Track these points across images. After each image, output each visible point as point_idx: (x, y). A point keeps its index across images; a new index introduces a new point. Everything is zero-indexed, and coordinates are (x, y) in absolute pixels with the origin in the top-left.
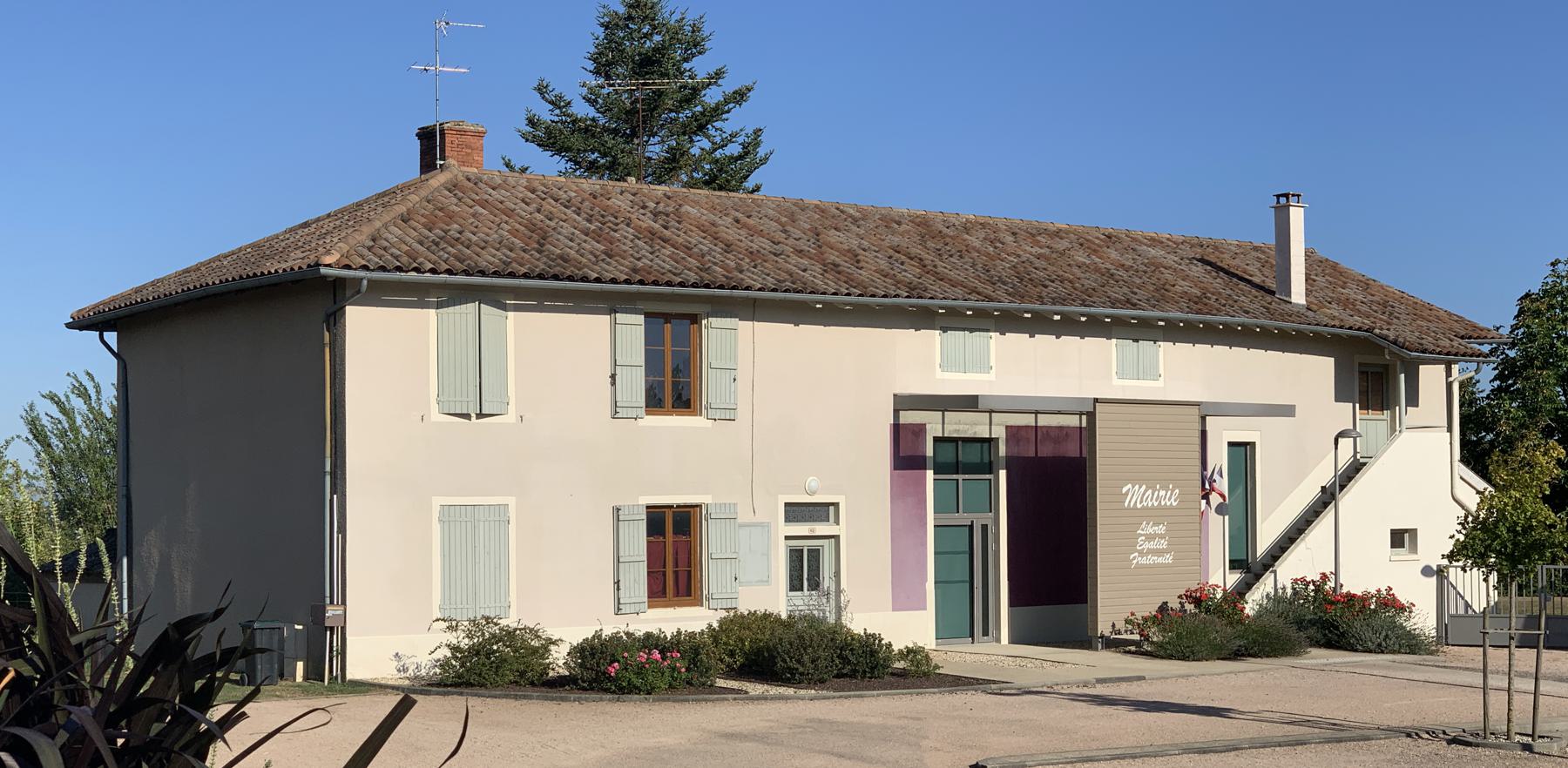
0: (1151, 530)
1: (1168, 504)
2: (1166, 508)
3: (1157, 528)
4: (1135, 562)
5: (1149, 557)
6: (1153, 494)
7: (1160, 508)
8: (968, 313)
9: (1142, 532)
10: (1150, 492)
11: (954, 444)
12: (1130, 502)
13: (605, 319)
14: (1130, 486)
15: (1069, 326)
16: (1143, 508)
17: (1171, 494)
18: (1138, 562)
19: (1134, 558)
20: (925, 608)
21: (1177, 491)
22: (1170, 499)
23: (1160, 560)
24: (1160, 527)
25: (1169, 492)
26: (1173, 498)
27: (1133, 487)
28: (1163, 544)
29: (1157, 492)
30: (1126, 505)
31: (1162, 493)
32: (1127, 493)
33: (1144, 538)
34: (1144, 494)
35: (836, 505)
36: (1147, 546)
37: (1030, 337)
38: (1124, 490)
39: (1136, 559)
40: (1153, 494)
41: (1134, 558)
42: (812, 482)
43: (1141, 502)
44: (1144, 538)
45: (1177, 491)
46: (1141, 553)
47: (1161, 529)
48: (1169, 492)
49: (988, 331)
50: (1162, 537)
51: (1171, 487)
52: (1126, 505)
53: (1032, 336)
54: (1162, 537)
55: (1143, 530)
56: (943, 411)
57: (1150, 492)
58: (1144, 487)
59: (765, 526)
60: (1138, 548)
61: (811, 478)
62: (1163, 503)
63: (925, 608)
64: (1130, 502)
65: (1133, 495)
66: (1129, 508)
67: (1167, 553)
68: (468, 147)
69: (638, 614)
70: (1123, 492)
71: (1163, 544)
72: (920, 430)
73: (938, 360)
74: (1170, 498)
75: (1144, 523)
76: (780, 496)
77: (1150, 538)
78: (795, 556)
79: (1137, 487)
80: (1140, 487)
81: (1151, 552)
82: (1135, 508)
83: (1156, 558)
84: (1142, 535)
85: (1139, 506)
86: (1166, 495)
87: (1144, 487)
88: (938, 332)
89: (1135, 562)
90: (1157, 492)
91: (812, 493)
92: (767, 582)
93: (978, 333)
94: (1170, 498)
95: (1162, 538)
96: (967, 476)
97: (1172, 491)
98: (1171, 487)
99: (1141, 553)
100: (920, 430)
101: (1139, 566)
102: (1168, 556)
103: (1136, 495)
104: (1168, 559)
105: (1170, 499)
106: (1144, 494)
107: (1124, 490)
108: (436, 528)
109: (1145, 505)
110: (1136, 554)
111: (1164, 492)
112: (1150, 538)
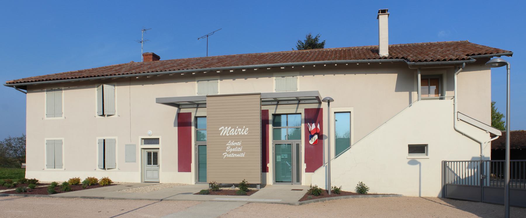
0: (233, 144)
2: (241, 135)
3: (237, 143)
4: (225, 156)
5: (232, 154)
6: (235, 130)
7: (238, 135)
9: (229, 145)
10: (233, 129)
11: (198, 118)
12: (223, 133)
14: (223, 127)
16: (230, 136)
17: (244, 130)
18: (226, 156)
19: (225, 155)
21: (247, 129)
22: (243, 132)
23: (238, 156)
25: (243, 129)
26: (245, 131)
27: (224, 128)
28: (240, 149)
29: (237, 130)
30: (221, 134)
31: (240, 130)
32: (221, 130)
33: (230, 147)
34: (230, 130)
35: (158, 139)
36: (231, 150)
37: (233, 80)
38: (220, 129)
39: (225, 155)
40: (235, 130)
41: (225, 155)
42: (150, 132)
43: (229, 133)
45: (247, 129)
46: (228, 153)
47: (239, 144)
48: (243, 129)
49: (218, 80)
50: (239, 147)
51: (244, 127)
54: (239, 147)
56: (197, 108)
57: (233, 129)
58: (230, 128)
59: (134, 146)
60: (227, 151)
61: (151, 132)
62: (240, 134)
64: (223, 133)
65: (225, 131)
66: (222, 136)
67: (242, 153)
68: (149, 58)
70: (219, 130)
71: (240, 149)
72: (190, 114)
74: (243, 131)
75: (230, 141)
76: (139, 136)
77: (232, 147)
79: (226, 128)
80: (228, 128)
81: (232, 152)
85: (227, 135)
86: (241, 130)
87: (230, 128)
88: (196, 82)
89: (225, 156)
90: (237, 130)
92: (135, 162)
93: (211, 81)
94: (243, 131)
95: (239, 147)
98: (244, 127)
99: (228, 153)
100: (190, 114)
101: (226, 158)
103: (225, 131)
104: (243, 155)
105: (243, 132)
106: (230, 130)
107: (220, 129)
109: (231, 134)
110: (226, 153)
111: (240, 130)
112: (232, 147)
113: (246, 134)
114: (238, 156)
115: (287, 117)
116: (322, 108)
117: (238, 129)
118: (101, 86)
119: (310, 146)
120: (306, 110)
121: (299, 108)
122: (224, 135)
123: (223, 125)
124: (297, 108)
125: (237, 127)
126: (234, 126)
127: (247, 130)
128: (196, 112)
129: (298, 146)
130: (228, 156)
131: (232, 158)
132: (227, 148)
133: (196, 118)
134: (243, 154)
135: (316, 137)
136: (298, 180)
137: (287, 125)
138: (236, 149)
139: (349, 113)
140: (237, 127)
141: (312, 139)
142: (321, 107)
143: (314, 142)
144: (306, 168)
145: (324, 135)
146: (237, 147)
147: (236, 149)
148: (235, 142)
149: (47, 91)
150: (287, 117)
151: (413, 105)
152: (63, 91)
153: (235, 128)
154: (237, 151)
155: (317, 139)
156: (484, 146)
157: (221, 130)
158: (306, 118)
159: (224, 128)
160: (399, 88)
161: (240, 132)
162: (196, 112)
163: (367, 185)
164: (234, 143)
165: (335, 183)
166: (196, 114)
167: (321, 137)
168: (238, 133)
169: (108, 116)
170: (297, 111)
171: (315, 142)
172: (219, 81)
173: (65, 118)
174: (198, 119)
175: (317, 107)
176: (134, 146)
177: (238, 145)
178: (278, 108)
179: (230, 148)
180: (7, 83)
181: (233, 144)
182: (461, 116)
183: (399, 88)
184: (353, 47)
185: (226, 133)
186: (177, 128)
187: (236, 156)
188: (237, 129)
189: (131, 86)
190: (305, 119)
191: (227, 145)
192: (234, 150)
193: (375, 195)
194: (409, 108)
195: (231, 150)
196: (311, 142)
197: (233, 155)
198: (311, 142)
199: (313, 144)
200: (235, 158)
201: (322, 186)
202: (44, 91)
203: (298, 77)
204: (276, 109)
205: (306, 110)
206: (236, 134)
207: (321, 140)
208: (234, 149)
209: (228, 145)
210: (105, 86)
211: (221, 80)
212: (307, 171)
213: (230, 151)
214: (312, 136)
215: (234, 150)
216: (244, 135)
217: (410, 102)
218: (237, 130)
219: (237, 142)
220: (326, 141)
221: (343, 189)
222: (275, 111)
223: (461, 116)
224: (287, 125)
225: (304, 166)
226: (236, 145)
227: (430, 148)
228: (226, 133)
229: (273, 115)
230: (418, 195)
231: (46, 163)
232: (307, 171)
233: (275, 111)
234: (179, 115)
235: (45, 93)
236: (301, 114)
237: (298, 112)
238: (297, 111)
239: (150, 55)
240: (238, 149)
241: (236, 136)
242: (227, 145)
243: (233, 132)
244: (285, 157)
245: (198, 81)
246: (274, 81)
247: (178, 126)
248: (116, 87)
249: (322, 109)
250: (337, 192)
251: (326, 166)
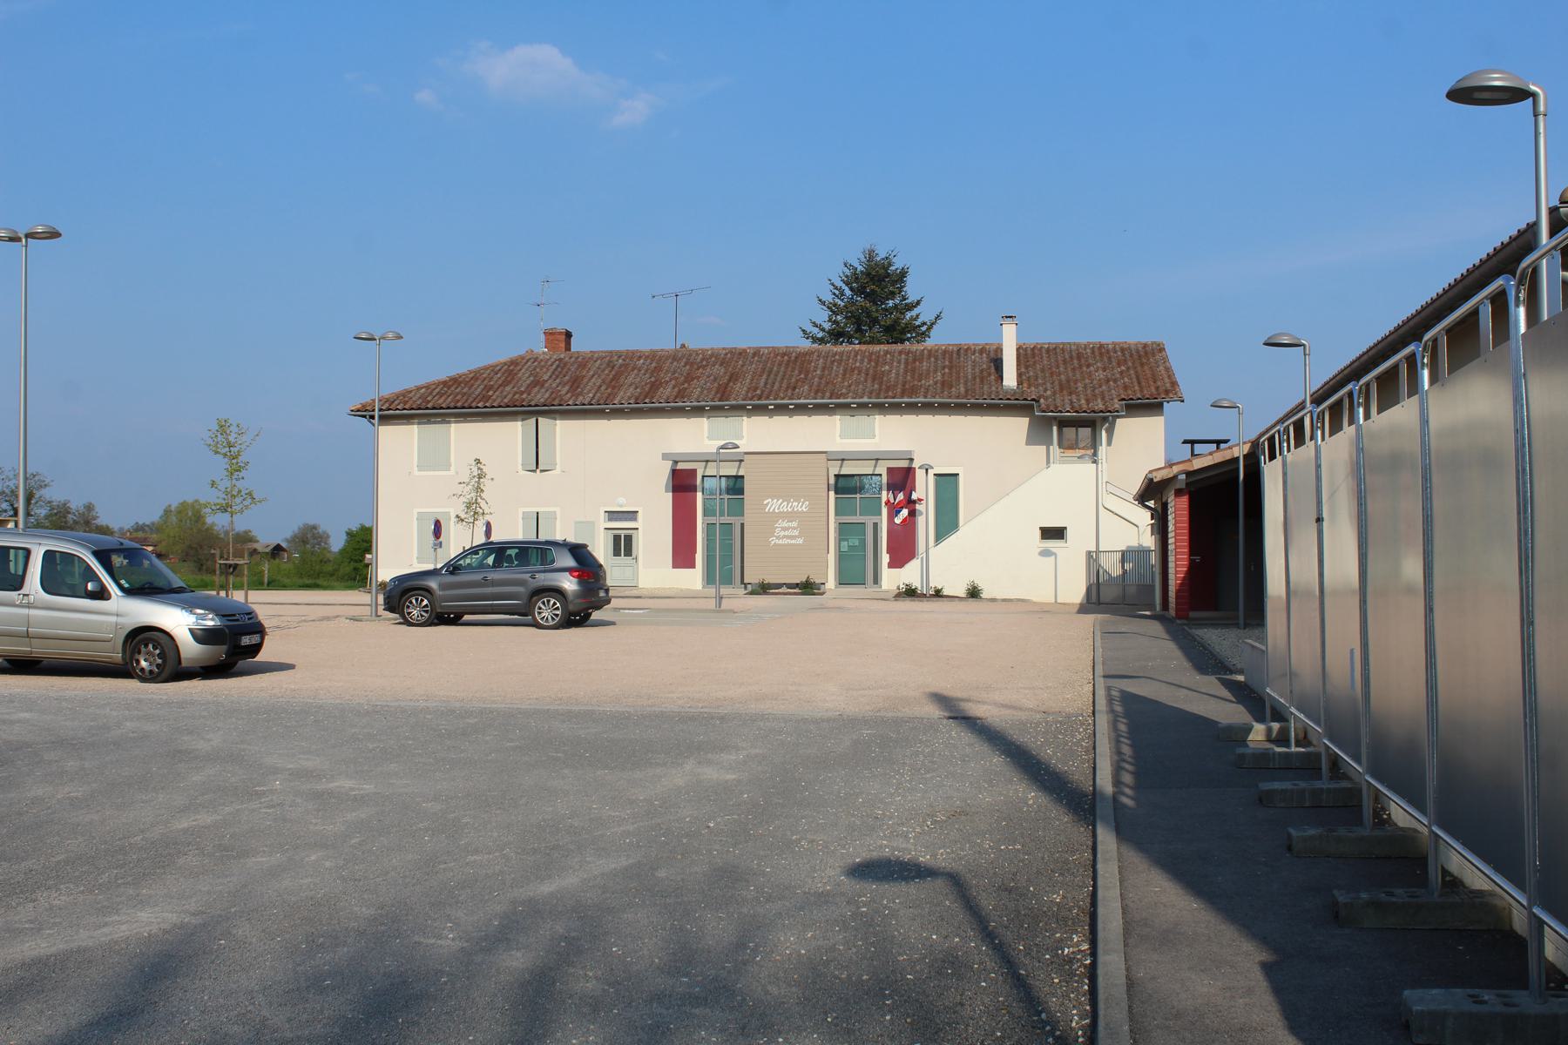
0: (785, 524)
2: (798, 512)
6: (788, 505)
8: (770, 407)
10: (786, 503)
14: (770, 500)
15: (912, 408)
20: (692, 565)
23: (793, 542)
28: (796, 533)
30: (767, 510)
32: (767, 504)
36: (782, 533)
38: (765, 502)
39: (773, 541)
40: (788, 505)
42: (622, 500)
46: (778, 538)
47: (794, 524)
52: (767, 510)
53: (901, 416)
57: (786, 503)
59: (593, 523)
63: (692, 565)
69: (974, 593)
71: (796, 533)
72: (694, 472)
73: (706, 434)
74: (803, 507)
77: (784, 529)
78: (617, 539)
81: (784, 537)
82: (774, 511)
85: (777, 511)
91: (621, 506)
94: (803, 507)
96: (731, 497)
97: (803, 503)
99: (778, 538)
100: (694, 472)
103: (774, 505)
104: (800, 541)
107: (765, 502)
108: (415, 522)
112: (784, 529)
114: (793, 542)
118: (534, 420)
120: (890, 470)
124: (875, 466)
126: (787, 499)
128: (705, 468)
129: (875, 525)
131: (784, 545)
133: (703, 477)
135: (905, 512)
136: (876, 580)
142: (913, 466)
149: (419, 424)
151: (1052, 465)
152: (453, 425)
156: (1141, 529)
158: (890, 482)
160: (1031, 441)
162: (705, 468)
163: (981, 585)
165: (935, 583)
166: (704, 472)
167: (913, 513)
169: (542, 471)
170: (874, 470)
171: (904, 520)
172: (745, 418)
173: (457, 473)
174: (705, 478)
176: (593, 523)
178: (844, 465)
180: (352, 411)
181: (785, 524)
182: (1111, 489)
183: (1031, 441)
184: (965, 345)
186: (671, 494)
189: (586, 421)
193: (993, 600)
194: (1045, 471)
195: (782, 533)
196: (898, 520)
197: (786, 541)
198: (898, 520)
200: (788, 545)
201: (916, 583)
202: (413, 424)
203: (877, 417)
204: (841, 467)
205: (890, 470)
206: (790, 510)
209: (777, 525)
210: (540, 419)
211: (749, 417)
212: (891, 565)
214: (898, 512)
216: (803, 512)
217: (1048, 462)
219: (792, 521)
220: (921, 520)
221: (945, 592)
222: (840, 470)
223: (1111, 489)
225: (885, 558)
227: (1069, 534)
229: (835, 475)
230: (1053, 601)
231: (415, 555)
232: (891, 565)
233: (840, 470)
234: (675, 473)
235: (416, 426)
236: (881, 475)
238: (874, 470)
239: (560, 333)
243: (786, 508)
245: (709, 417)
246: (838, 423)
247: (674, 491)
248: (558, 422)
250: (938, 594)
251: (922, 558)
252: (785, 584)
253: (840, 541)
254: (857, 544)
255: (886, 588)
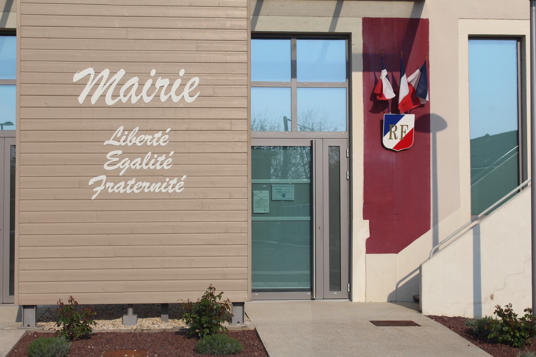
1: (176, 99)
2: (170, 106)
3: (150, 137)
4: (99, 189)
5: (130, 183)
7: (156, 106)
9: (116, 143)
12: (90, 96)
13: (290, 40)
14: (90, 71)
16: (119, 107)
17: (183, 85)
19: (98, 183)
21: (196, 80)
23: (156, 188)
24: (158, 135)
25: (178, 82)
27: (97, 73)
29: (149, 83)
30: (81, 99)
32: (82, 83)
33: (120, 152)
34: (121, 84)
36: (126, 165)
38: (77, 77)
41: (98, 183)
43: (114, 96)
44: (120, 152)
45: (196, 80)
46: (113, 176)
48: (178, 82)
50: (158, 151)
51: (182, 72)
54: (158, 151)
55: (118, 139)
57: (135, 80)
58: (121, 73)
60: (106, 167)
62: (163, 98)
64: (90, 96)
65: (97, 84)
66: (87, 106)
67: (172, 177)
79: (106, 73)
80: (112, 73)
81: (131, 174)
82: (101, 105)
83: (148, 184)
84: (113, 147)
85: (109, 101)
86: (171, 85)
87: (121, 73)
89: (99, 189)
90: (149, 83)
95: (160, 154)
98: (182, 72)
99: (113, 176)
101: (105, 196)
102: (175, 181)
105: (178, 93)
106: (121, 84)
107: (77, 77)
110: (103, 177)
111: (166, 82)
113: (189, 100)
114: (156, 188)
115: (293, 48)
116: (427, 20)
117: (155, 79)
119: (384, 156)
121: (342, 12)
122: (94, 100)
123: (91, 62)
124: (337, 15)
125: (153, 72)
127: (192, 85)
130: (110, 191)
132: (108, 156)
134: (179, 181)
137: (294, 74)
138: (145, 161)
139: (514, 42)
140: (153, 72)
141: (393, 129)
142: (423, 16)
143: (398, 141)
144: (368, 236)
145: (434, 115)
146: (150, 154)
147: (145, 161)
148: (142, 131)
150: (293, 48)
153: (144, 77)
154: (152, 167)
155: (411, 132)
157: (82, 83)
158: (371, 51)
159: (97, 73)
161: (166, 94)
164: (137, 135)
168: (157, 96)
170: (334, 24)
175: (409, 17)
177: (155, 144)
179: (121, 157)
185: (103, 96)
187: (146, 190)
188: (150, 77)
190: (366, 56)
191: (106, 143)
192: (137, 164)
195: (126, 165)
199: (397, 147)
200: (143, 197)
206: (147, 100)
207: (423, 134)
208: (139, 160)
209: (111, 142)
213: (119, 169)
215: (137, 164)
218: (153, 85)
219: (153, 131)
224: (294, 74)
226: (149, 143)
228: (103, 96)
236: (347, 36)
237: (340, 29)
238: (334, 24)
240: (156, 161)
241: (147, 107)
242: (106, 143)
244: (284, 195)
249: (426, 21)
252: (131, 305)
253: (255, 187)
254: (291, 196)
255: (363, 300)
